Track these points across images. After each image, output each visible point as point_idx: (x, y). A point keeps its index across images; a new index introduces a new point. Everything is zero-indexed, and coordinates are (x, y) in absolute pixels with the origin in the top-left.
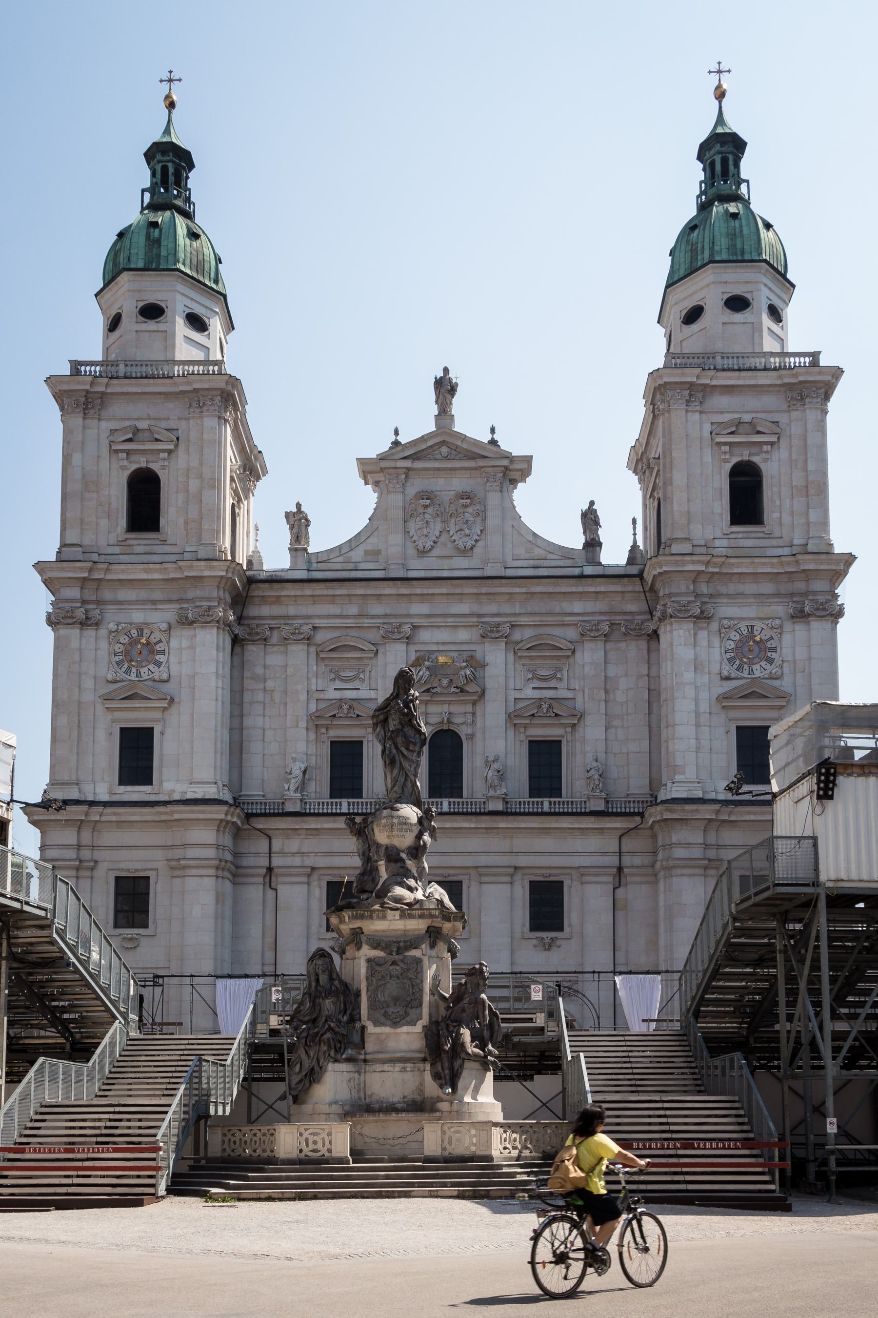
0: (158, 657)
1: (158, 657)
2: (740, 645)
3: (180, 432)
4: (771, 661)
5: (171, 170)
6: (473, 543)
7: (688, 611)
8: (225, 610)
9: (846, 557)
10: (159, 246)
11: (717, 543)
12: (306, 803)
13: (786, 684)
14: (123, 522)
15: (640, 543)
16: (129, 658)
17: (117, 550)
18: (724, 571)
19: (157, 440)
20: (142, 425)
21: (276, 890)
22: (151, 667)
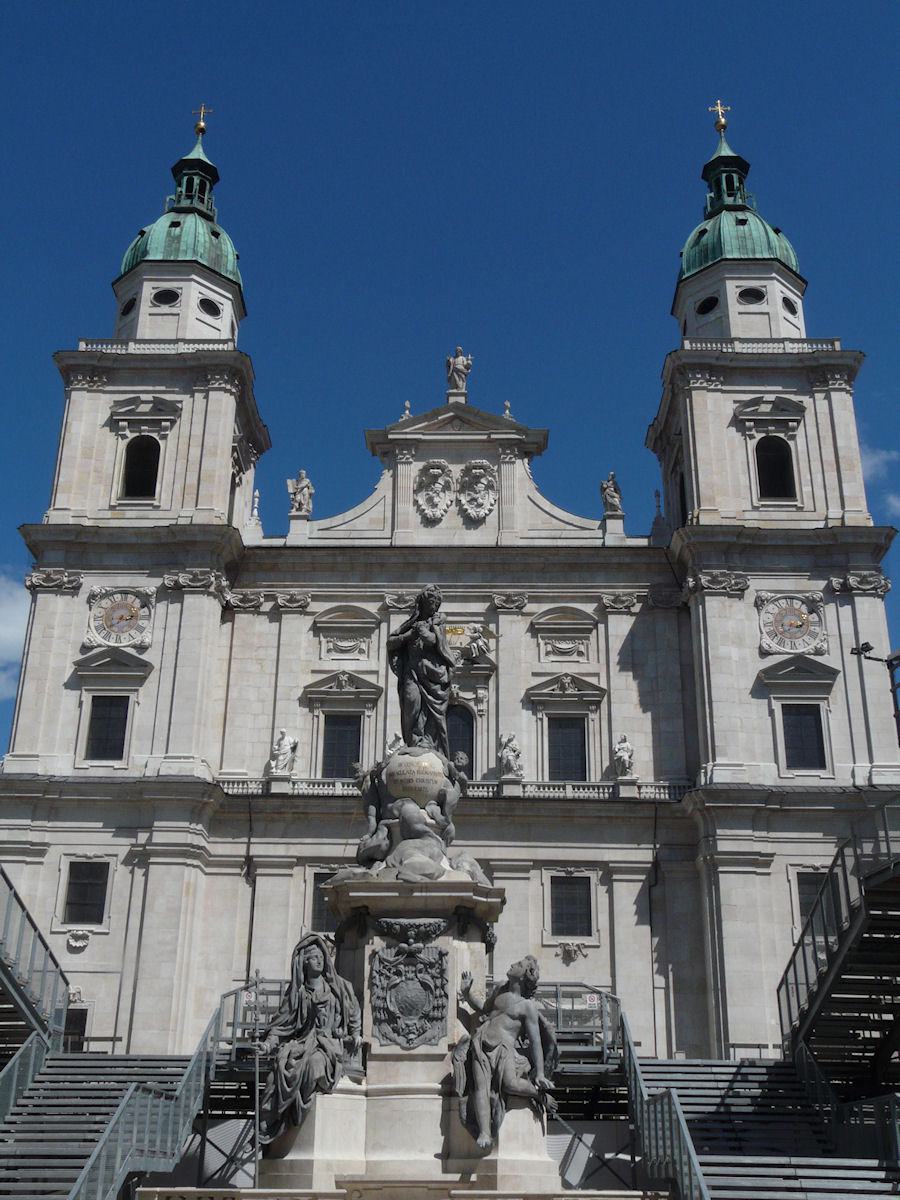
0: (140, 623)
1: (140, 623)
2: (779, 618)
3: (184, 403)
4: (814, 635)
5: (197, 180)
6: (487, 512)
7: (721, 583)
8: (217, 577)
9: (887, 531)
10: (179, 242)
11: (748, 515)
12: (294, 783)
13: (831, 660)
14: (118, 487)
15: (663, 516)
16: (109, 624)
17: (109, 514)
18: (757, 543)
19: (160, 410)
20: (144, 397)
21: (254, 882)
22: (133, 632)
